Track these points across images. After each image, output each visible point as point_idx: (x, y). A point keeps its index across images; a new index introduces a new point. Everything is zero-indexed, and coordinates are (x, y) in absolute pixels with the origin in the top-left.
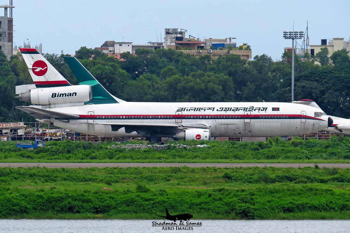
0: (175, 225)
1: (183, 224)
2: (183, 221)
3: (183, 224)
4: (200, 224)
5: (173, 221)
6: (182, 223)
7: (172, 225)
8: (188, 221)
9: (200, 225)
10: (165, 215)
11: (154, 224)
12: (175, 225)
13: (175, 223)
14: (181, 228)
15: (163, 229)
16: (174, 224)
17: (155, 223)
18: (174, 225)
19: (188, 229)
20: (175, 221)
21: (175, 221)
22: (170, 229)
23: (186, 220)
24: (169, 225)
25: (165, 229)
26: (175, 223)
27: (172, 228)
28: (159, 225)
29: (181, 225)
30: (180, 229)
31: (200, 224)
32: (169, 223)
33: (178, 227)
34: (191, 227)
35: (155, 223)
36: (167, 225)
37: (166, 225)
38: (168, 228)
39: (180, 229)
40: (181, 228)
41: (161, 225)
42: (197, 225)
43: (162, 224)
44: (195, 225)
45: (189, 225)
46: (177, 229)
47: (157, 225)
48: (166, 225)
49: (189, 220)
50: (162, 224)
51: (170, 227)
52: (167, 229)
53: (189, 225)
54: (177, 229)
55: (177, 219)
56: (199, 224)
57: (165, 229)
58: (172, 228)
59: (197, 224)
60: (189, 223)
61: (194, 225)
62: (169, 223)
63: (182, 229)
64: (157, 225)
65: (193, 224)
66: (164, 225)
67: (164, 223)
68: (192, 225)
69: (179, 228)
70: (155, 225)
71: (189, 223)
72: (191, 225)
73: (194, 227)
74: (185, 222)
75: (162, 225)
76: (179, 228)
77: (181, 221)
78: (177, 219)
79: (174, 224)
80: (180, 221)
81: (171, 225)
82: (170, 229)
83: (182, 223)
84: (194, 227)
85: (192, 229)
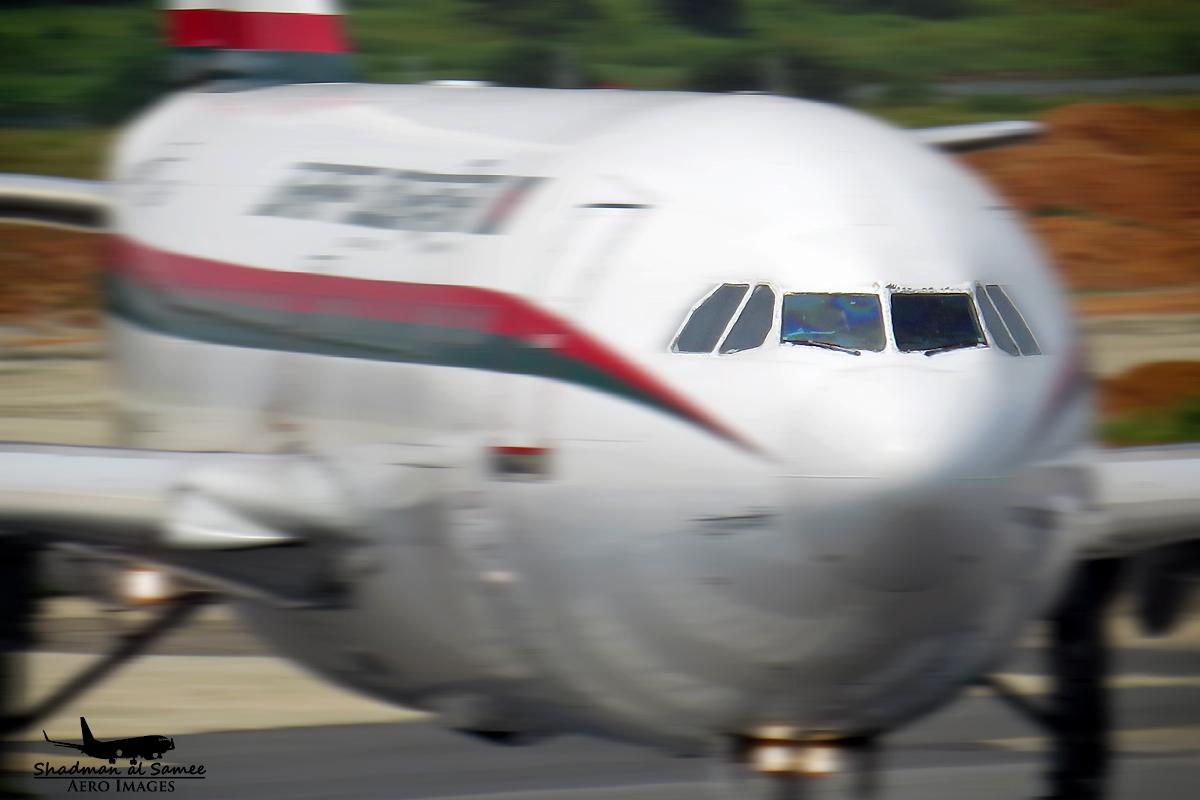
0: (114, 774)
2: (139, 760)
5: (105, 763)
6: (137, 766)
7: (104, 775)
9: (197, 775)
10: (83, 744)
12: (114, 774)
14: (132, 785)
15: (72, 789)
18: (108, 775)
19: (158, 789)
20: (112, 761)
21: (112, 761)
22: (96, 787)
23: (149, 757)
24: (92, 774)
25: (79, 789)
27: (104, 787)
30: (128, 789)
32: (94, 768)
34: (168, 781)
35: (44, 768)
36: (87, 774)
37: (81, 775)
38: (87, 784)
39: (128, 789)
41: (64, 775)
42: (189, 775)
44: (183, 774)
45: (160, 775)
47: (51, 774)
48: (81, 775)
49: (160, 757)
50: (70, 771)
51: (97, 781)
52: (84, 788)
54: (118, 789)
55: (119, 753)
56: (196, 770)
57: (79, 789)
58: (104, 787)
61: (177, 775)
62: (94, 768)
63: (136, 787)
65: (174, 770)
66: (76, 775)
67: (76, 767)
68: (171, 775)
70: (43, 775)
72: (167, 775)
73: (177, 783)
75: (68, 775)
78: (119, 753)
79: (111, 770)
80: (132, 762)
81: (98, 775)
82: (96, 787)
84: (177, 783)
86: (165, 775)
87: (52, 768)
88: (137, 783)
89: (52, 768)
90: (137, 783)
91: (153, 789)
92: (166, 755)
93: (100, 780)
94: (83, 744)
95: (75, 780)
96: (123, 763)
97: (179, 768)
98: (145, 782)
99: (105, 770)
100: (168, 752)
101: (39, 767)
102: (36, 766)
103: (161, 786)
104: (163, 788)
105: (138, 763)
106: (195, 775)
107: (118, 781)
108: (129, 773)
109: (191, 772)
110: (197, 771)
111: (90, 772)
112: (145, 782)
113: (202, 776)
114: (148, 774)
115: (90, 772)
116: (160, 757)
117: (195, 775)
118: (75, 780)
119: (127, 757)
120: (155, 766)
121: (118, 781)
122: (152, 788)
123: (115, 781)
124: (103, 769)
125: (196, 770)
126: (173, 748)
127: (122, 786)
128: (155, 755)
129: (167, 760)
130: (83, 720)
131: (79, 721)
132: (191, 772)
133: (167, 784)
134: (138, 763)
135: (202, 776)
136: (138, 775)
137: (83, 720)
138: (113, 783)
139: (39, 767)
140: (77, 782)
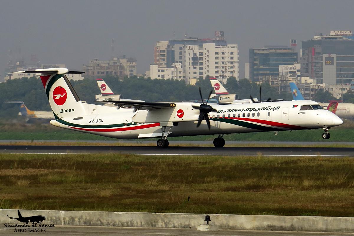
2: (35, 223)
4: (53, 226)
5: (25, 223)
7: (25, 227)
8: (41, 223)
10: (18, 218)
12: (28, 227)
14: (33, 230)
15: (16, 231)
16: (27, 226)
17: (7, 225)
18: (26, 227)
21: (27, 223)
24: (21, 227)
25: (17, 231)
27: (25, 230)
28: (11, 227)
30: (32, 231)
36: (20, 227)
39: (32, 231)
40: (33, 230)
41: (13, 227)
42: (50, 227)
43: (15, 226)
46: (29, 232)
48: (18, 227)
49: (41, 222)
50: (15, 226)
55: (29, 221)
56: (52, 226)
57: (17, 231)
58: (25, 230)
59: (49, 226)
67: (17, 225)
68: (45, 227)
69: (31, 230)
70: (7, 227)
71: (42, 225)
72: (43, 227)
74: (38, 224)
75: (14, 227)
76: (31, 230)
77: (33, 223)
79: (27, 226)
81: (23, 227)
83: (34, 225)
92: (43, 221)
96: (30, 224)
101: (6, 225)
102: (5, 225)
107: (29, 229)
109: (50, 226)
116: (41, 222)
119: (32, 222)
121: (29, 229)
123: (28, 229)
127: (30, 231)
128: (40, 221)
129: (44, 222)
138: (27, 230)
139: (6, 225)
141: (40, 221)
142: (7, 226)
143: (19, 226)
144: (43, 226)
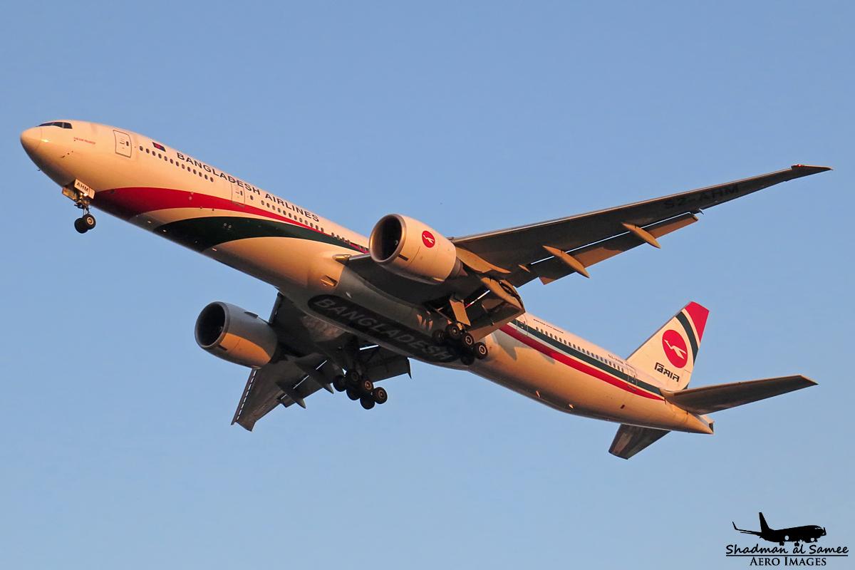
0: (783, 553)
1: (801, 550)
2: (801, 542)
3: (801, 550)
4: (843, 551)
5: (777, 544)
6: (799, 548)
7: (776, 553)
8: (814, 543)
9: (842, 554)
10: (760, 531)
11: (732, 551)
12: (783, 553)
13: (782, 547)
14: (796, 560)
15: (753, 564)
16: (781, 550)
17: (733, 549)
18: (779, 553)
19: (815, 563)
20: (782, 544)
21: (782, 544)
22: (771, 562)
23: (808, 541)
24: (768, 553)
25: (758, 564)
26: (783, 547)
28: (742, 554)
29: (796, 554)
30: (793, 564)
31: (843, 551)
32: (769, 549)
33: (789, 558)
34: (822, 558)
35: (733, 549)
36: (764, 553)
37: (759, 553)
39: (793, 564)
40: (796, 560)
41: (747, 554)
42: (837, 554)
43: (752, 551)
44: (832, 553)
45: (816, 554)
46: (786, 564)
47: (738, 553)
48: (759, 553)
49: (816, 541)
50: (752, 551)
51: (771, 558)
52: (762, 563)
53: (816, 554)
54: (786, 564)
55: (787, 538)
56: (841, 550)
57: (758, 564)
60: (816, 549)
61: (828, 553)
62: (769, 549)
63: (799, 562)
64: (738, 553)
65: (826, 550)
66: (756, 553)
67: (756, 548)
68: (824, 553)
69: (791, 560)
70: (733, 554)
71: (816, 549)
72: (821, 553)
73: (828, 559)
74: (806, 546)
75: (751, 554)
76: (791, 560)
77: (797, 544)
78: (787, 538)
79: (781, 550)
80: (796, 545)
81: (771, 554)
82: (771, 562)
83: (799, 548)
84: (828, 559)
85: (824, 564)
86: (819, 554)
87: (739, 549)
88: (799, 559)
89: (739, 549)
90: (799, 559)
91: (811, 564)
93: (774, 557)
94: (760, 531)
95: (755, 557)
96: (789, 546)
97: (829, 549)
98: (805, 559)
99: (776, 550)
100: (822, 537)
101: (729, 548)
103: (817, 562)
104: (818, 563)
105: (800, 545)
106: (841, 554)
107: (786, 558)
108: (794, 552)
109: (838, 551)
110: (842, 551)
111: (766, 552)
112: (805, 559)
113: (846, 554)
114: (807, 553)
115: (762, 552)
116: (816, 541)
117: (841, 554)
118: (755, 557)
119: (793, 541)
120: (812, 548)
121: (786, 558)
122: (810, 563)
123: (784, 558)
124: (775, 550)
125: (841, 550)
126: (825, 534)
128: (812, 539)
129: (822, 542)
130: (761, 514)
131: (759, 515)
132: (838, 551)
133: (821, 560)
134: (800, 545)
135: (846, 554)
136: (800, 553)
137: (761, 514)
138: (782, 559)
139: (729, 548)
140: (757, 559)
141: (812, 539)
142: (732, 551)
143: (761, 550)
144: (820, 550)
